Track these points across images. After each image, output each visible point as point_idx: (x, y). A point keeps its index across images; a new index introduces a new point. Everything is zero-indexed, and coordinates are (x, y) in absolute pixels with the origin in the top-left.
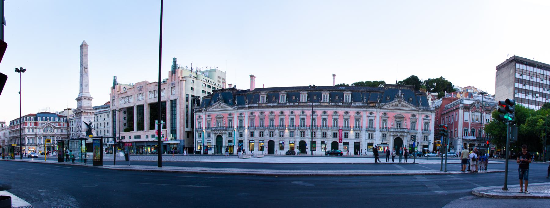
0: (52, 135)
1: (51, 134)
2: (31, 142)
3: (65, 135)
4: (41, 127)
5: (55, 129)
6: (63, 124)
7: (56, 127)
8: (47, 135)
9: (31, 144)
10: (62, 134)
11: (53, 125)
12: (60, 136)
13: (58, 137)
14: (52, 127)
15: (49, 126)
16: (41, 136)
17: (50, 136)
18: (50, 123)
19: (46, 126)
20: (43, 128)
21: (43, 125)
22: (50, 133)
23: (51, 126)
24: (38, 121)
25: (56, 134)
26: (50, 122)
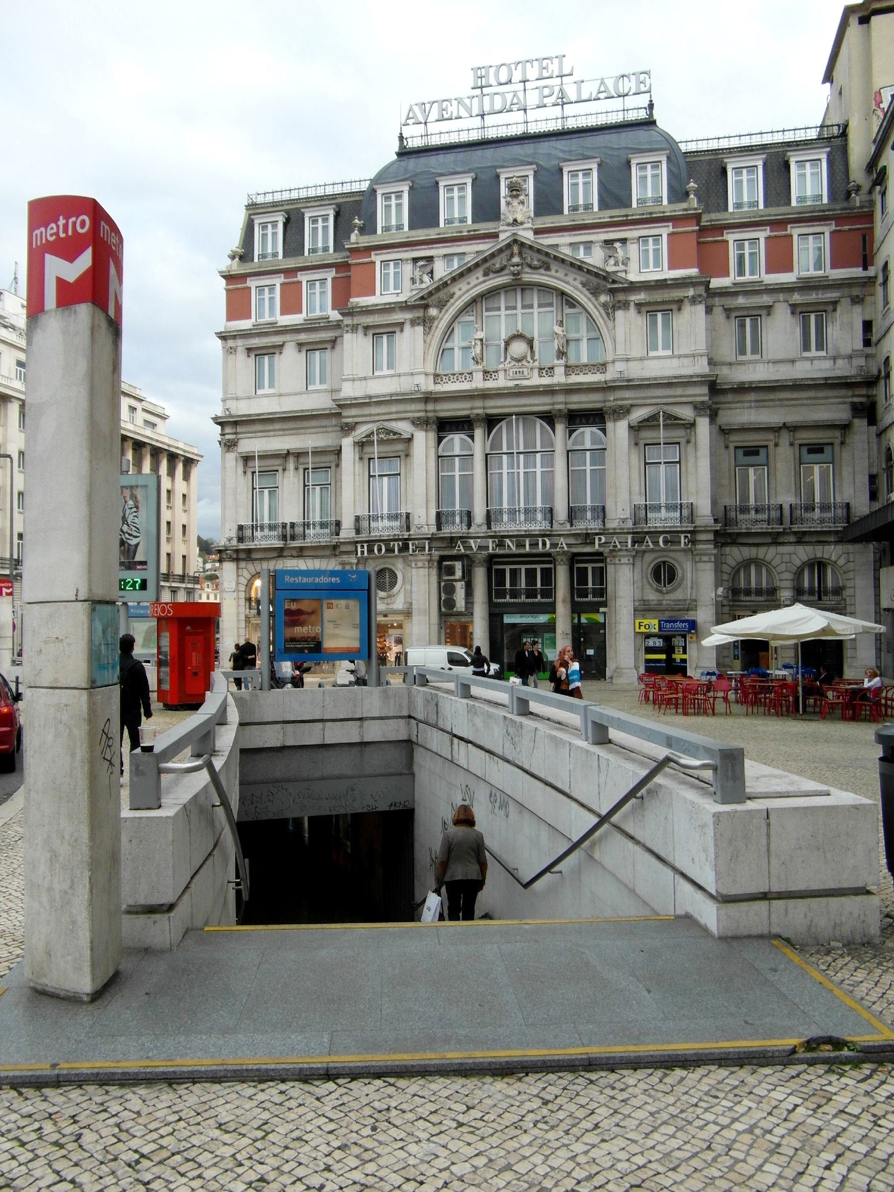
0: (559, 403)
1: (549, 391)
2: (290, 513)
3: (797, 386)
4: (405, 307)
5: (610, 310)
6: (762, 235)
7: (634, 287)
8: (477, 408)
9: (288, 532)
10: (742, 389)
11: (578, 267)
12: (699, 408)
13: (649, 423)
14: (572, 285)
15: (518, 286)
16: (404, 428)
17: (549, 418)
18: (547, 241)
19: (477, 284)
20: (427, 323)
21: (441, 270)
22: (536, 380)
23: (555, 278)
24: (365, 241)
25: (630, 385)
26: (549, 221)
